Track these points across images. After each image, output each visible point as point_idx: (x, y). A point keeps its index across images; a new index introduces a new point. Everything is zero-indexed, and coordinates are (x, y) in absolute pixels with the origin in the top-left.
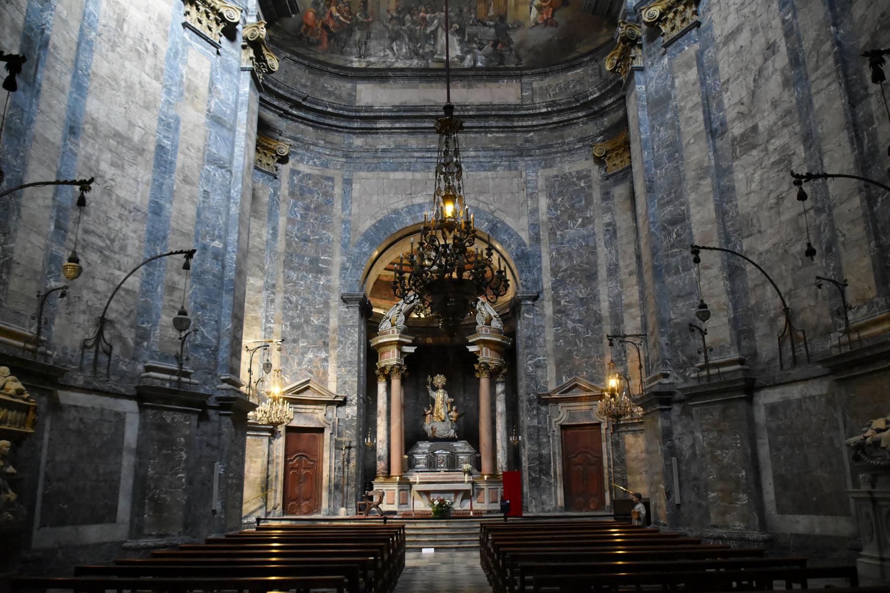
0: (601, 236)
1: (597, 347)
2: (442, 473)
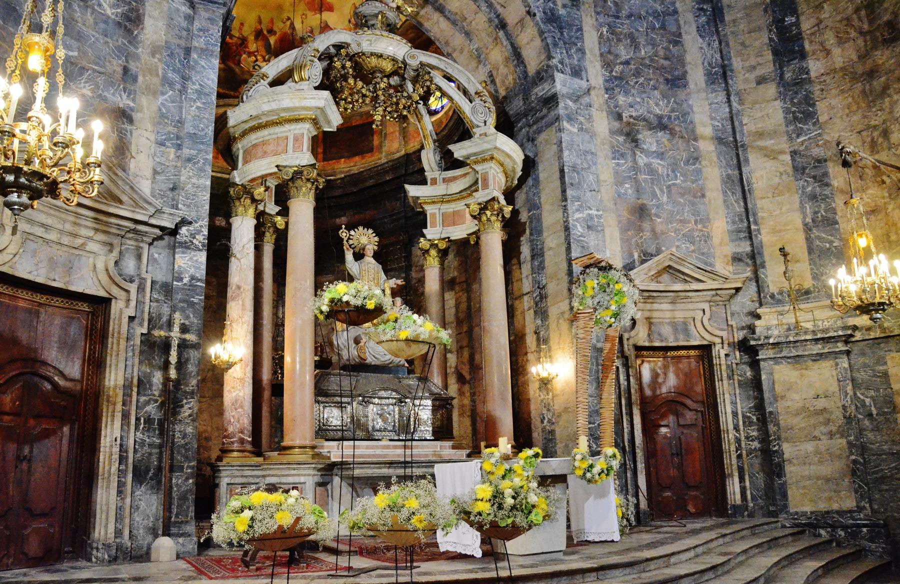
0: (690, 17)
1: (693, 204)
2: (384, 443)
